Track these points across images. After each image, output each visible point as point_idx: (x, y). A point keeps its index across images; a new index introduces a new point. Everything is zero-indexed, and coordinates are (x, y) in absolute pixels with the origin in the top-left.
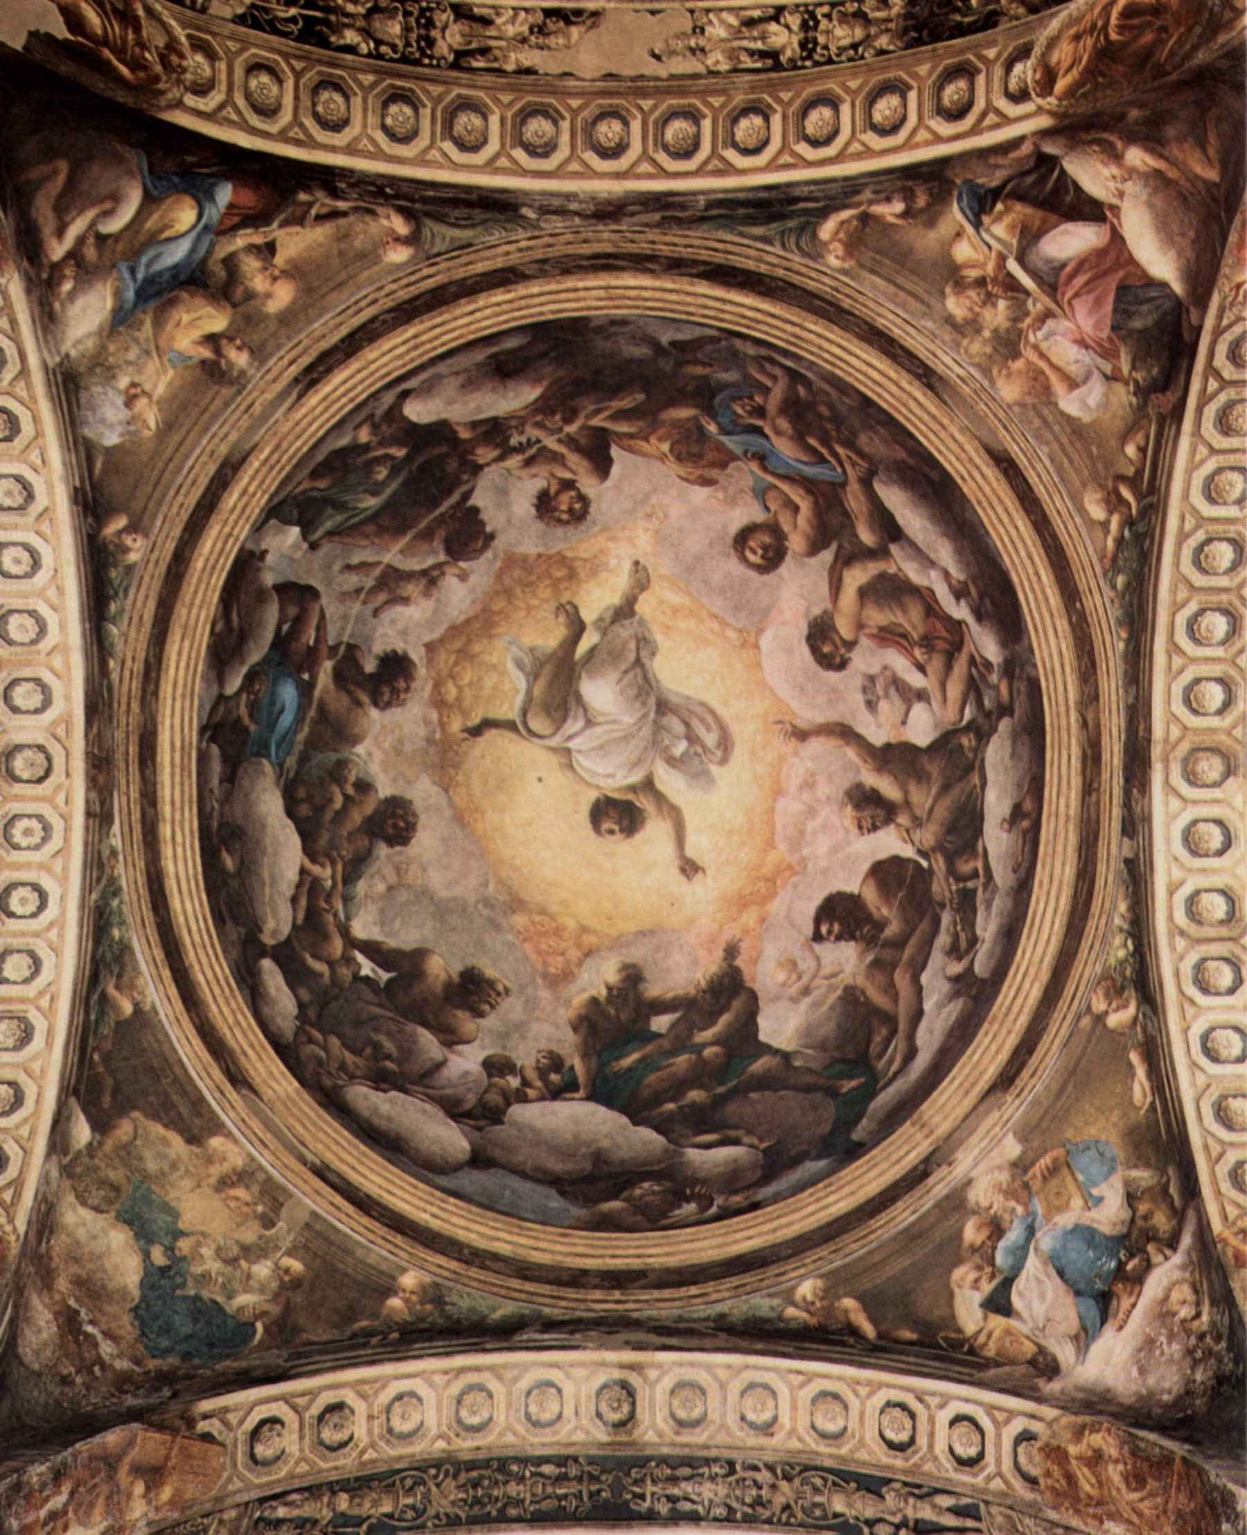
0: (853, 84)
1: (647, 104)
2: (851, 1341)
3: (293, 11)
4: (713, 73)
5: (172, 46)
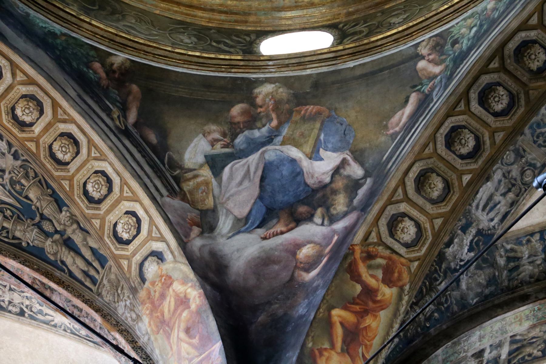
2: (116, 113)
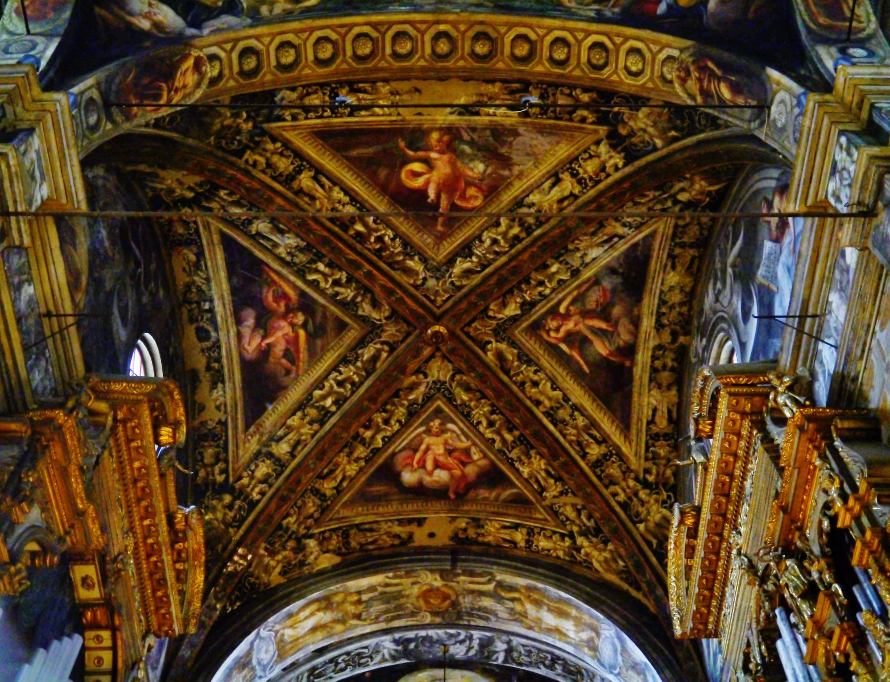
0: (307, 71)
1: (422, 63)
3: (616, 109)
4: (386, 81)
5: (683, 81)
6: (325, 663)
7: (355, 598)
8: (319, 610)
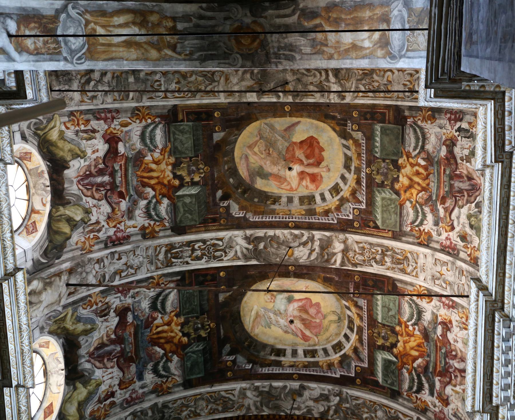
6: (183, 245)
7: (170, 24)
8: (134, 23)
